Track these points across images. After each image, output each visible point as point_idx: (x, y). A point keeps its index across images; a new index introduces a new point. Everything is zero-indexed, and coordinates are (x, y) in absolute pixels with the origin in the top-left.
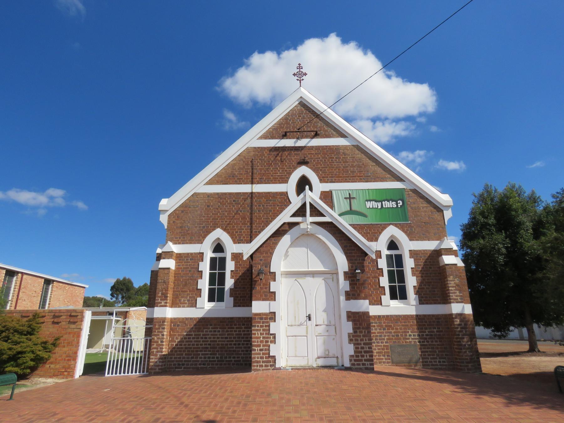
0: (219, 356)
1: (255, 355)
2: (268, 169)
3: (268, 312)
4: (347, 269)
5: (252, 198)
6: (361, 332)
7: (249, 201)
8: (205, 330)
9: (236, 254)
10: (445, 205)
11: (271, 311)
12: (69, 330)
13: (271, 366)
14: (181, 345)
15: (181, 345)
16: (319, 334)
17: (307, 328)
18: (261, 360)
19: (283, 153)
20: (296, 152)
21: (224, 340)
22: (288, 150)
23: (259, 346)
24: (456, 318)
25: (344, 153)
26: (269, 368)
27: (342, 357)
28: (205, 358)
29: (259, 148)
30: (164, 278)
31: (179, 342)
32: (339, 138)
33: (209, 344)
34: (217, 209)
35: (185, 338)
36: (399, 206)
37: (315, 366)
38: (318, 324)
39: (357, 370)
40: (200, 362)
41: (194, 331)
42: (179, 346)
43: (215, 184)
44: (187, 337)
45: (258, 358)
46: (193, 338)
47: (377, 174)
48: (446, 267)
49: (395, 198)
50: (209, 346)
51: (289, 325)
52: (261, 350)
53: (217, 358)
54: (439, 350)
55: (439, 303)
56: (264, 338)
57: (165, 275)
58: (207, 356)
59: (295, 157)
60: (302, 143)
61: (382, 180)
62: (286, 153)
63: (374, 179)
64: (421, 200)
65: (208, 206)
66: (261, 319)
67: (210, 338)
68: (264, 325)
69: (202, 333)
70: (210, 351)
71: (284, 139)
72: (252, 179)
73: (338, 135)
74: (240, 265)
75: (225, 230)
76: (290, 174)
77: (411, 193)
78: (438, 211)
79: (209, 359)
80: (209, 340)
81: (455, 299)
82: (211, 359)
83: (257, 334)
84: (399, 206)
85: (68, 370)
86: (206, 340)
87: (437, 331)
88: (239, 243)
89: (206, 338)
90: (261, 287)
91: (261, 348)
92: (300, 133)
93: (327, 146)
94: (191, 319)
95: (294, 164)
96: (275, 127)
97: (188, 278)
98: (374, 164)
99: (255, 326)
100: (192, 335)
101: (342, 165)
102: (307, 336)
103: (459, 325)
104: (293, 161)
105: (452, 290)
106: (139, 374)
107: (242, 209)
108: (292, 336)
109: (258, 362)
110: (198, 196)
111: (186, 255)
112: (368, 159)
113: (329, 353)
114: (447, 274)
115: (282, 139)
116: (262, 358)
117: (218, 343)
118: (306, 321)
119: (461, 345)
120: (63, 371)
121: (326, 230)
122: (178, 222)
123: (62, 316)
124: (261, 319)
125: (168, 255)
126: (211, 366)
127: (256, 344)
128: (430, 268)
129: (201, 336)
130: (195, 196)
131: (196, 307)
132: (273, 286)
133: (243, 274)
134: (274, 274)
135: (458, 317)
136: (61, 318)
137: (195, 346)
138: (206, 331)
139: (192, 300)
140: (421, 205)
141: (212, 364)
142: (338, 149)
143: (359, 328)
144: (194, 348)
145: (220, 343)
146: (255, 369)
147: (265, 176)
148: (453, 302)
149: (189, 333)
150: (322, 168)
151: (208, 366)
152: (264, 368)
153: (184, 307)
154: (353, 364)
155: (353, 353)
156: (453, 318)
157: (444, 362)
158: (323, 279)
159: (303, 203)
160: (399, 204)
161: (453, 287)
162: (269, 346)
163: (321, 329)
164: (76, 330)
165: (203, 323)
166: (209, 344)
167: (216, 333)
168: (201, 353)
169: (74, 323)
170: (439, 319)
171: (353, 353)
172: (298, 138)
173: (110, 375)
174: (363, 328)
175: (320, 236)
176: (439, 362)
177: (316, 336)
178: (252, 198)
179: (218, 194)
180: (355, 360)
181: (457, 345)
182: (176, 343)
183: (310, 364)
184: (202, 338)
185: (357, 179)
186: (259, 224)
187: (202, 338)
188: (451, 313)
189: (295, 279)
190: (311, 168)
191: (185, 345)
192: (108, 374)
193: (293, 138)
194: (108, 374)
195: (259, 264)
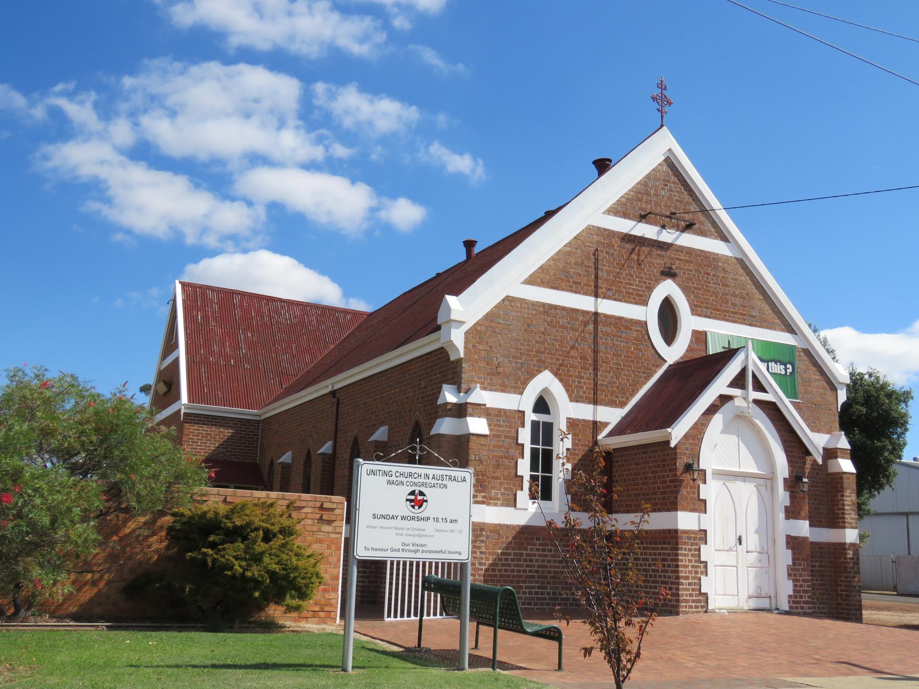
0: (551, 591)
1: (684, 591)
2: (619, 273)
3: (697, 528)
4: (787, 476)
5: (596, 323)
6: (800, 565)
7: (591, 327)
8: (529, 547)
9: (574, 420)
10: (841, 381)
11: (702, 528)
12: (321, 536)
13: (702, 607)
14: (494, 570)
15: (494, 570)
16: (750, 564)
17: (737, 555)
18: (690, 598)
19: (642, 248)
20: (659, 252)
21: (558, 564)
22: (648, 245)
23: (687, 578)
24: (849, 549)
25: (723, 269)
26: (700, 609)
27: (776, 597)
28: (530, 593)
29: (605, 230)
30: (480, 452)
31: (491, 565)
32: (718, 240)
33: (537, 572)
34: (543, 333)
35: (500, 559)
36: (788, 374)
37: (746, 608)
38: (749, 550)
39: (798, 614)
40: (523, 601)
41: (514, 549)
42: (490, 573)
43: (539, 285)
44: (503, 557)
45: (686, 596)
46: (513, 560)
47: (763, 314)
48: (844, 476)
49: (785, 361)
50: (535, 574)
51: (716, 550)
52: (690, 584)
53: (549, 593)
54: (820, 592)
55: (824, 526)
56: (693, 567)
57: (480, 448)
58: (533, 590)
59: (658, 261)
60: (667, 236)
61: (769, 326)
62: (645, 249)
63: (761, 323)
64: (814, 368)
65: (529, 325)
66: (689, 538)
67: (537, 561)
68: (693, 548)
69: (525, 552)
70: (537, 582)
71: (643, 222)
72: (596, 287)
73: (717, 235)
74: (579, 440)
75: (556, 374)
76: (650, 289)
77: (802, 354)
78: (832, 390)
79: (536, 596)
80: (536, 564)
81: (851, 523)
82: (539, 596)
83: (685, 558)
84: (788, 374)
85: (327, 609)
86: (532, 563)
87: (819, 566)
88: (577, 401)
89: (531, 561)
90: (687, 491)
91: (690, 581)
92: (668, 220)
93: (701, 251)
94: (507, 526)
95: (656, 272)
96: (630, 197)
97: (500, 454)
98: (761, 297)
99: (682, 549)
100: (510, 554)
101: (720, 289)
102: (737, 567)
103: (852, 559)
104: (655, 267)
105: (847, 510)
106: (441, 617)
107: (581, 340)
108: (720, 566)
109: (687, 601)
110: (513, 304)
111: (496, 412)
112: (754, 288)
113: (761, 590)
114: (844, 487)
115: (640, 221)
116: (691, 595)
117: (549, 569)
118: (736, 545)
119: (852, 586)
120: (317, 609)
121: (764, 412)
122: (481, 347)
123: (304, 507)
124: (689, 538)
125: (481, 410)
126: (539, 607)
127: (683, 575)
128: (818, 474)
129: (525, 557)
130: (507, 303)
131: (515, 506)
132: (705, 491)
133: (584, 456)
134: (703, 472)
135: (852, 548)
136: (302, 511)
137: (515, 573)
138: (532, 549)
139: (508, 495)
140: (814, 377)
141: (542, 604)
142: (717, 259)
143: (798, 559)
144: (513, 576)
145: (552, 570)
146: (684, 611)
147: (614, 286)
148: (848, 528)
149: (505, 551)
150: (695, 288)
151: (536, 607)
152: (693, 610)
153: (495, 505)
154: (791, 607)
155: (791, 593)
156: (845, 549)
157: (823, 608)
158: (755, 486)
159: (743, 367)
160: (788, 370)
161: (849, 505)
162: (700, 579)
163: (753, 557)
164: (333, 536)
165: (526, 534)
166: (537, 572)
167: (546, 553)
168: (524, 585)
169: (329, 522)
170: (822, 548)
171: (791, 593)
172: (663, 227)
173: (432, 617)
174: (802, 560)
175: (758, 422)
176: (819, 608)
177: (748, 567)
178: (596, 323)
179: (543, 305)
180: (794, 602)
181: (846, 586)
182: (486, 567)
183: (741, 605)
184: (525, 560)
185: (739, 318)
186: (607, 372)
187: (525, 560)
188: (842, 541)
189: (722, 482)
190: (679, 285)
191: (500, 570)
192: (389, 616)
193: (656, 225)
194: (389, 616)
195: (685, 454)
